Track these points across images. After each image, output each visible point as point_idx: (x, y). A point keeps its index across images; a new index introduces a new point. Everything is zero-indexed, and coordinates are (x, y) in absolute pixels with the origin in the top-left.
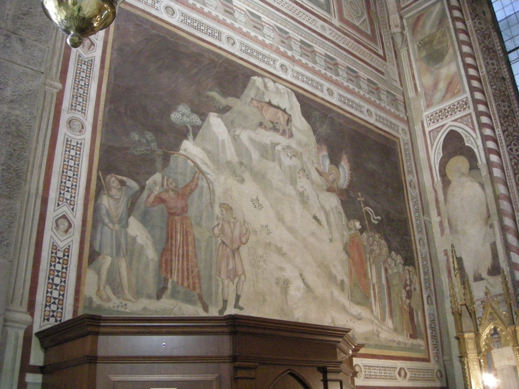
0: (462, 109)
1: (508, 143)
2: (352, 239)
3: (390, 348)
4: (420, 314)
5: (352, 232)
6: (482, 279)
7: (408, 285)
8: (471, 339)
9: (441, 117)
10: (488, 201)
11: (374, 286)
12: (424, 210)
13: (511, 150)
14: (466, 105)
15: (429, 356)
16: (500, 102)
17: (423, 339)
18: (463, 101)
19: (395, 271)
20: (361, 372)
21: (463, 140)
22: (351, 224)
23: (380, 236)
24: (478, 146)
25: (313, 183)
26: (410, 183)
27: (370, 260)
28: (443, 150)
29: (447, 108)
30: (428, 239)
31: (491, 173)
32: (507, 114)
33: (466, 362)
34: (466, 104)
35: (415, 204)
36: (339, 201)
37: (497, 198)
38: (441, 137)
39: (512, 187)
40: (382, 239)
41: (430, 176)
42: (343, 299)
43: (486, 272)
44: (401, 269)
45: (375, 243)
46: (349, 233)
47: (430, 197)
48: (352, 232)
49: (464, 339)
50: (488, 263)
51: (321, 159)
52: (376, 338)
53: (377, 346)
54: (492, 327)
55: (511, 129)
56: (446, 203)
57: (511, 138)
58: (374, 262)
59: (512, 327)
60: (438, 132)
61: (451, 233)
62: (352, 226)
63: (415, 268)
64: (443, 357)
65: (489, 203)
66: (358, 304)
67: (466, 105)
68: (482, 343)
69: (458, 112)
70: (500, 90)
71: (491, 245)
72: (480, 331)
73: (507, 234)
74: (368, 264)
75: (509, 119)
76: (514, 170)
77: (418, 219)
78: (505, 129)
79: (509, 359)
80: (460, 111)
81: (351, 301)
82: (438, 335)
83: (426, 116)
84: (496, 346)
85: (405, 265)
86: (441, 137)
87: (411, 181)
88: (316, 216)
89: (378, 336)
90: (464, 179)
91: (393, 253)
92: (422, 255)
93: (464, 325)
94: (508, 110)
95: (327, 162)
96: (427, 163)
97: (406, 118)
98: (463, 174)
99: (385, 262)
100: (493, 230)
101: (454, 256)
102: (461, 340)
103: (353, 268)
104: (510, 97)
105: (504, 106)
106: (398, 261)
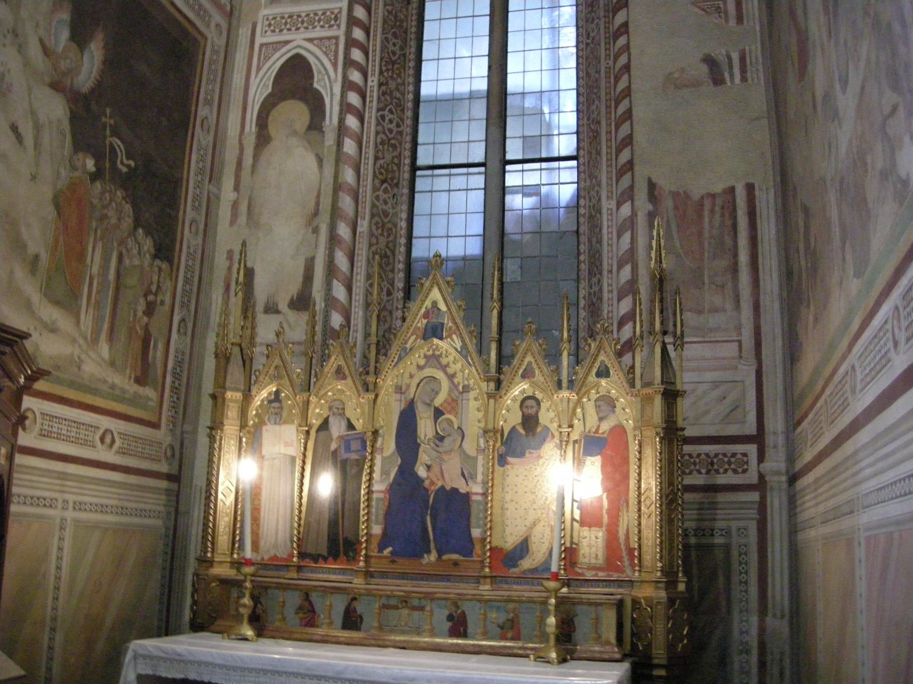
0: (327, 26)
1: (382, 105)
2: (73, 186)
3: (95, 392)
4: (161, 346)
5: (77, 174)
6: (277, 312)
7: (151, 292)
8: (236, 401)
9: (288, 26)
10: (322, 188)
11: (91, 278)
12: (214, 175)
13: (383, 117)
14: (336, 21)
15: (160, 419)
16: (390, 36)
17: (155, 390)
18: (332, 13)
19: (137, 262)
20: (35, 422)
21: (312, 77)
22: (78, 159)
23: (124, 195)
24: (332, 95)
25: (26, 63)
26: (203, 121)
27: (96, 231)
28: (274, 83)
29: (303, 15)
30: (206, 225)
31: (339, 144)
32: (394, 59)
33: (218, 438)
34: (336, 19)
35: (202, 159)
36: (68, 113)
37: (337, 187)
38: (278, 60)
39: (365, 177)
40: (127, 202)
41: (239, 120)
42: (31, 290)
43: (287, 302)
44: (146, 263)
45: (114, 205)
46: (71, 174)
47: (230, 155)
48: (77, 174)
49: (224, 399)
50: (294, 288)
51: (54, 24)
52: (76, 370)
53: (72, 385)
54: (274, 389)
55: (392, 85)
56: (253, 173)
57: (388, 98)
58: (102, 239)
59: (306, 395)
60: (276, 50)
62: (79, 164)
63: (171, 265)
64: (183, 424)
65: (322, 192)
66: (57, 303)
67: (336, 21)
68: (252, 411)
69: (318, 28)
70: (396, 17)
71: (306, 260)
72: (253, 392)
74: (92, 239)
75: (395, 67)
76: (377, 151)
77: (198, 186)
78: (382, 80)
79: (287, 444)
80: (322, 27)
81: (45, 295)
82: (183, 390)
83: (264, 16)
84: (273, 422)
85: (155, 257)
86: (278, 60)
87: (206, 118)
88: (16, 124)
89: (79, 368)
90: (294, 141)
91: (140, 231)
92: (189, 247)
93: (229, 377)
94: (398, 52)
95: (65, 34)
96: (241, 98)
97: (228, 8)
98: (295, 133)
99: (122, 243)
101: (243, 261)
102: (220, 400)
103: (61, 238)
104: (409, 33)
105: (394, 45)
106: (146, 248)
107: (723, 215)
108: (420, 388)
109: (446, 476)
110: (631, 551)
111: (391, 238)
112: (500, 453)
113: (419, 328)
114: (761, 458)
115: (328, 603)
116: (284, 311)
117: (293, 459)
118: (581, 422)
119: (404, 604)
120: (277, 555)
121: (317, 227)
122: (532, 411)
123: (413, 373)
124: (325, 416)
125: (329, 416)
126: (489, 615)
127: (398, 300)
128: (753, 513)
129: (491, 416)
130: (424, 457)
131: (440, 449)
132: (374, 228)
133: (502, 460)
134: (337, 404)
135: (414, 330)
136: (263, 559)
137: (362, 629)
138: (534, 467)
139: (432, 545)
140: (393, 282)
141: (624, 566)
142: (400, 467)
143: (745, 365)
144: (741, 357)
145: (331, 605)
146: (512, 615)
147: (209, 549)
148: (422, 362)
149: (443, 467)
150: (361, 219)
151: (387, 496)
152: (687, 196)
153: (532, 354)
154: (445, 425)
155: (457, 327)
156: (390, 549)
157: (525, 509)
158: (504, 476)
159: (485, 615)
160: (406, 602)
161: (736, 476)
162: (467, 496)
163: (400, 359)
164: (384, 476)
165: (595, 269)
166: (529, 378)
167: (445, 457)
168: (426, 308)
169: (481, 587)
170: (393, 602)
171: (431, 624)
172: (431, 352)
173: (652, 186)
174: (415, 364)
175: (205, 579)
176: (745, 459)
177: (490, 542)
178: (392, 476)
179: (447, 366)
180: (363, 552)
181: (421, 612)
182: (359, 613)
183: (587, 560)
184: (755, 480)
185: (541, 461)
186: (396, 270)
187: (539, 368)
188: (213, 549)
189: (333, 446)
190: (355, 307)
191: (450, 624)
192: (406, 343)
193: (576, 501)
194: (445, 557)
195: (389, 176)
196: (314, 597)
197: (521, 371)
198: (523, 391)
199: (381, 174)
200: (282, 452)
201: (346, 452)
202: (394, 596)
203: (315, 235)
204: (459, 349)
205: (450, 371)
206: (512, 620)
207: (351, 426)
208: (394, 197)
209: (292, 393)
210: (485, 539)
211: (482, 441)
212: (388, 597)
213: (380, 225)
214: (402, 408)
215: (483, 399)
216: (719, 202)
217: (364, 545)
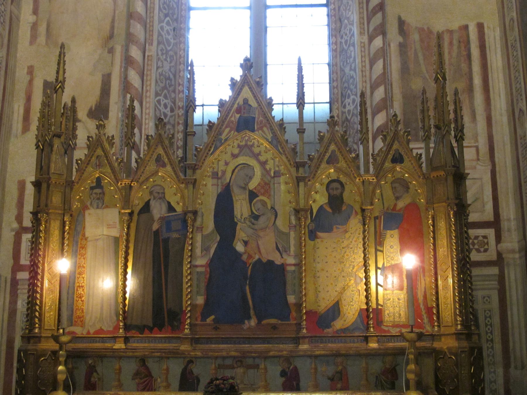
10: (116, 15)
30: (9, 41)
43: (86, 112)
61: (47, 44)
65: (116, 18)
71: (103, 76)
73: (130, 69)
79: (109, 226)
84: (95, 206)
100: (113, 55)
101: (62, 61)
107: (459, 47)
108: (234, 174)
109: (263, 251)
110: (429, 310)
111: (172, 64)
112: (310, 229)
113: (232, 122)
114: (498, 239)
115: (165, 367)
116: (83, 120)
117: (116, 240)
118: (381, 200)
119: (239, 364)
120: (103, 328)
121: (112, 48)
122: (337, 192)
123: (228, 161)
124: (146, 201)
125: (150, 200)
126: (319, 369)
127: (179, 116)
128: (495, 284)
130: (241, 234)
131: (256, 227)
132: (160, 53)
133: (313, 236)
134: (157, 189)
136: (88, 333)
137: (199, 389)
138: (341, 241)
139: (252, 312)
140: (175, 101)
141: (424, 323)
142: (219, 243)
143: (482, 166)
144: (478, 159)
145: (167, 369)
147: (37, 325)
148: (236, 151)
149: (259, 242)
150: (149, 45)
151: (208, 270)
152: (430, 32)
153: (336, 144)
154: (259, 205)
155: (268, 120)
156: (213, 317)
157: (335, 277)
158: (315, 248)
159: (316, 369)
160: (241, 362)
161: (479, 254)
162: (282, 267)
163: (216, 148)
165: (349, 91)
166: (333, 164)
167: (261, 234)
168: (238, 104)
170: (228, 362)
171: (266, 381)
172: (243, 143)
173: (401, 23)
174: (229, 154)
175: (33, 354)
176: (486, 241)
177: (305, 307)
178: (212, 251)
179: (259, 154)
180: (188, 321)
181: (256, 370)
182: (196, 375)
183: (391, 319)
184: (494, 257)
185: (347, 235)
186: (177, 91)
187: (342, 155)
188: (40, 325)
189: (155, 227)
190: (146, 119)
191: (284, 379)
192: (221, 134)
193: (380, 269)
194: (264, 322)
195: (171, 12)
196: (150, 364)
197: (325, 160)
199: (165, 9)
200: (105, 233)
202: (231, 357)
203: (111, 55)
204: (270, 140)
205: (262, 158)
206: (340, 373)
207: (171, 208)
208: (174, 30)
209: (114, 180)
210: (301, 305)
211: (293, 218)
212: (224, 358)
213: (164, 52)
214: (219, 191)
216: (456, 36)
217: (189, 315)
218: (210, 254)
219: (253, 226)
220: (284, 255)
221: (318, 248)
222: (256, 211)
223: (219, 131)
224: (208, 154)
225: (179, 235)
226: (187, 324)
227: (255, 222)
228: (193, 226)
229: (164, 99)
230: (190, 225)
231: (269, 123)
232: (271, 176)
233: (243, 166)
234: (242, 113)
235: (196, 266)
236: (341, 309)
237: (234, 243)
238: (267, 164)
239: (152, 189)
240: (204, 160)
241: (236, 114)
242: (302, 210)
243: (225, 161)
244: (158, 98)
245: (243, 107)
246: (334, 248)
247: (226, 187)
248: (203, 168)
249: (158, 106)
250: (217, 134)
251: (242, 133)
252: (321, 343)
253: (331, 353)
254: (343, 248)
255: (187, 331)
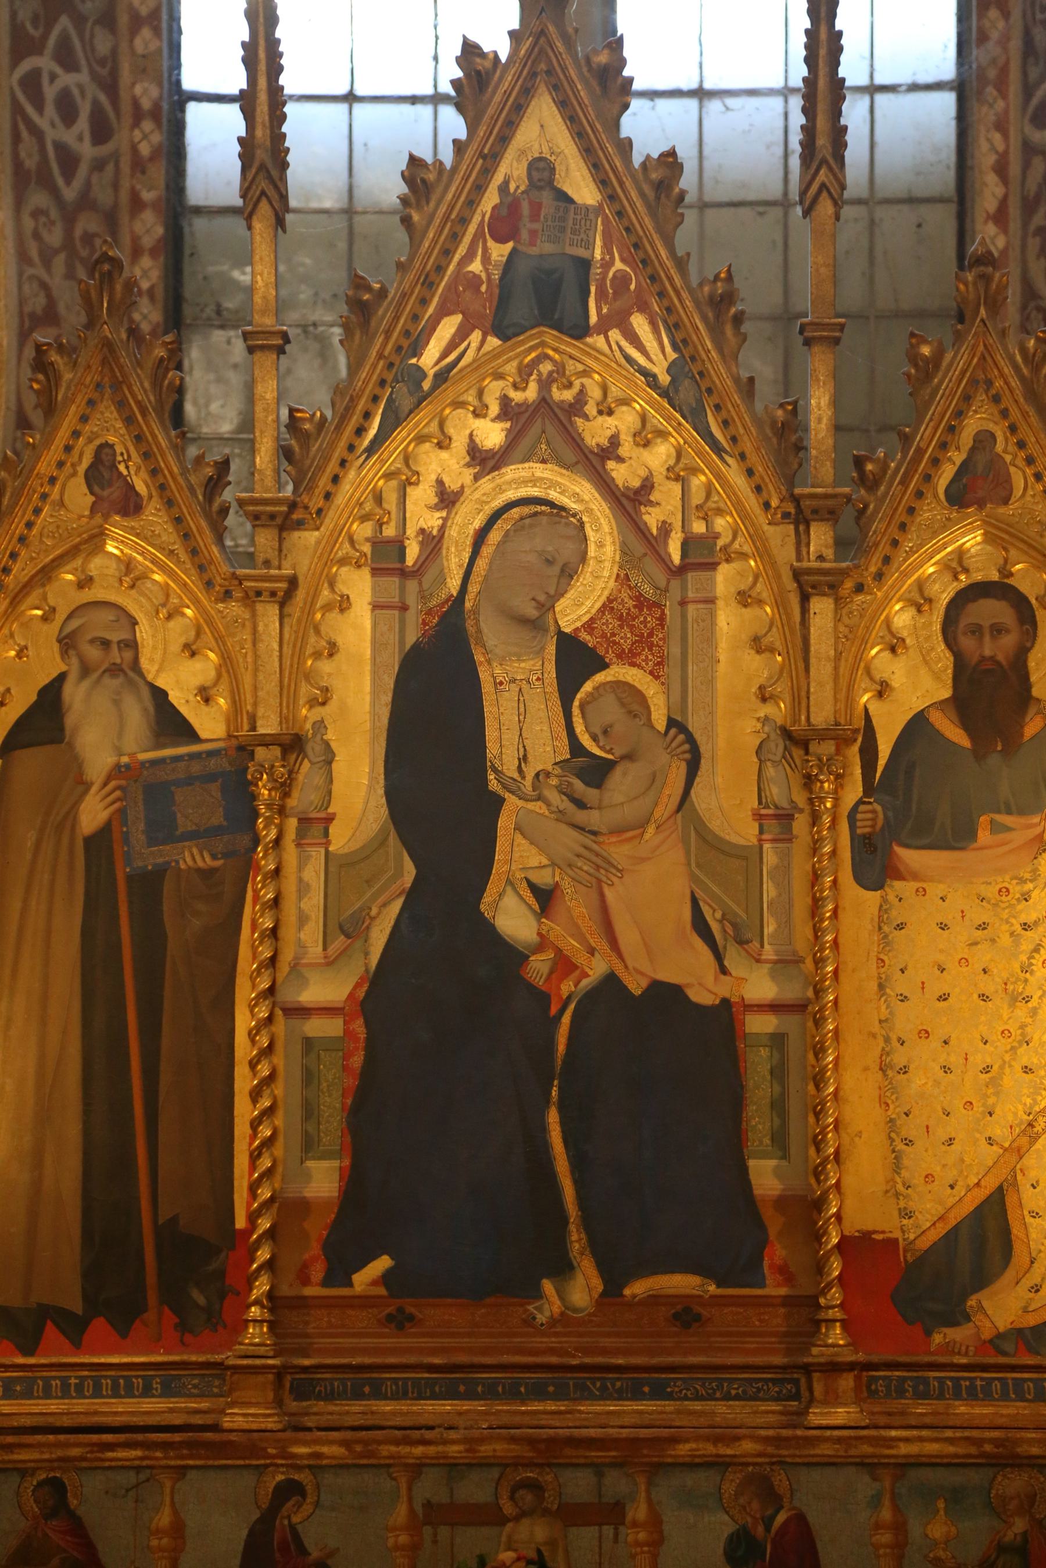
108: (487, 551)
109: (628, 936)
113: (474, 281)
115: (165, 1519)
119: (527, 1498)
123: (452, 484)
124: (44, 680)
125: (62, 677)
126: (915, 1529)
129: (821, 671)
131: (593, 818)
134: (100, 624)
135: (452, 287)
138: (1016, 890)
139: (576, 1239)
140: (114, 74)
142: (413, 896)
145: (178, 1529)
146: (1020, 1525)
151: (359, 1026)
154: (610, 711)
155: (653, 278)
156: (383, 1263)
157: (987, 1070)
159: (899, 1527)
160: (535, 1487)
163: (393, 421)
164: (339, 942)
166: (981, 504)
167: (619, 852)
168: (503, 188)
169: (817, 1416)
172: (532, 393)
174: (459, 443)
177: (838, 1216)
178: (379, 938)
179: (611, 450)
180: (261, 1287)
181: (608, 1531)
182: (315, 1554)
186: (123, 20)
192: (417, 350)
194: (637, 1289)
197: (943, 481)
198: (958, 563)
201: (152, 841)
202: (484, 1464)
204: (664, 379)
205: (621, 474)
210: (819, 1204)
212: (453, 1469)
214: (412, 638)
215: (781, 604)
217: (263, 1254)
218: (367, 954)
219: (581, 816)
220: (733, 958)
221: (900, 927)
222: (594, 738)
223: (407, 333)
224: (351, 448)
225: (214, 857)
226: (257, 1302)
227: (591, 794)
228: (282, 811)
229: (58, 70)
230: (269, 807)
231: (662, 294)
232: (664, 560)
233: (526, 510)
234: (525, 235)
235: (303, 1012)
236: (1016, 1231)
237: (487, 898)
238: (651, 503)
239: (74, 624)
240: (336, 479)
241: (491, 243)
242: (823, 735)
243: (440, 482)
244: (26, 65)
245: (525, 209)
246: (983, 927)
247: (444, 617)
248: (329, 522)
249: (30, 110)
250: (399, 349)
251: (526, 349)
252: (923, 1395)
253: (973, 1450)
254: (1026, 927)
255: (255, 1335)
